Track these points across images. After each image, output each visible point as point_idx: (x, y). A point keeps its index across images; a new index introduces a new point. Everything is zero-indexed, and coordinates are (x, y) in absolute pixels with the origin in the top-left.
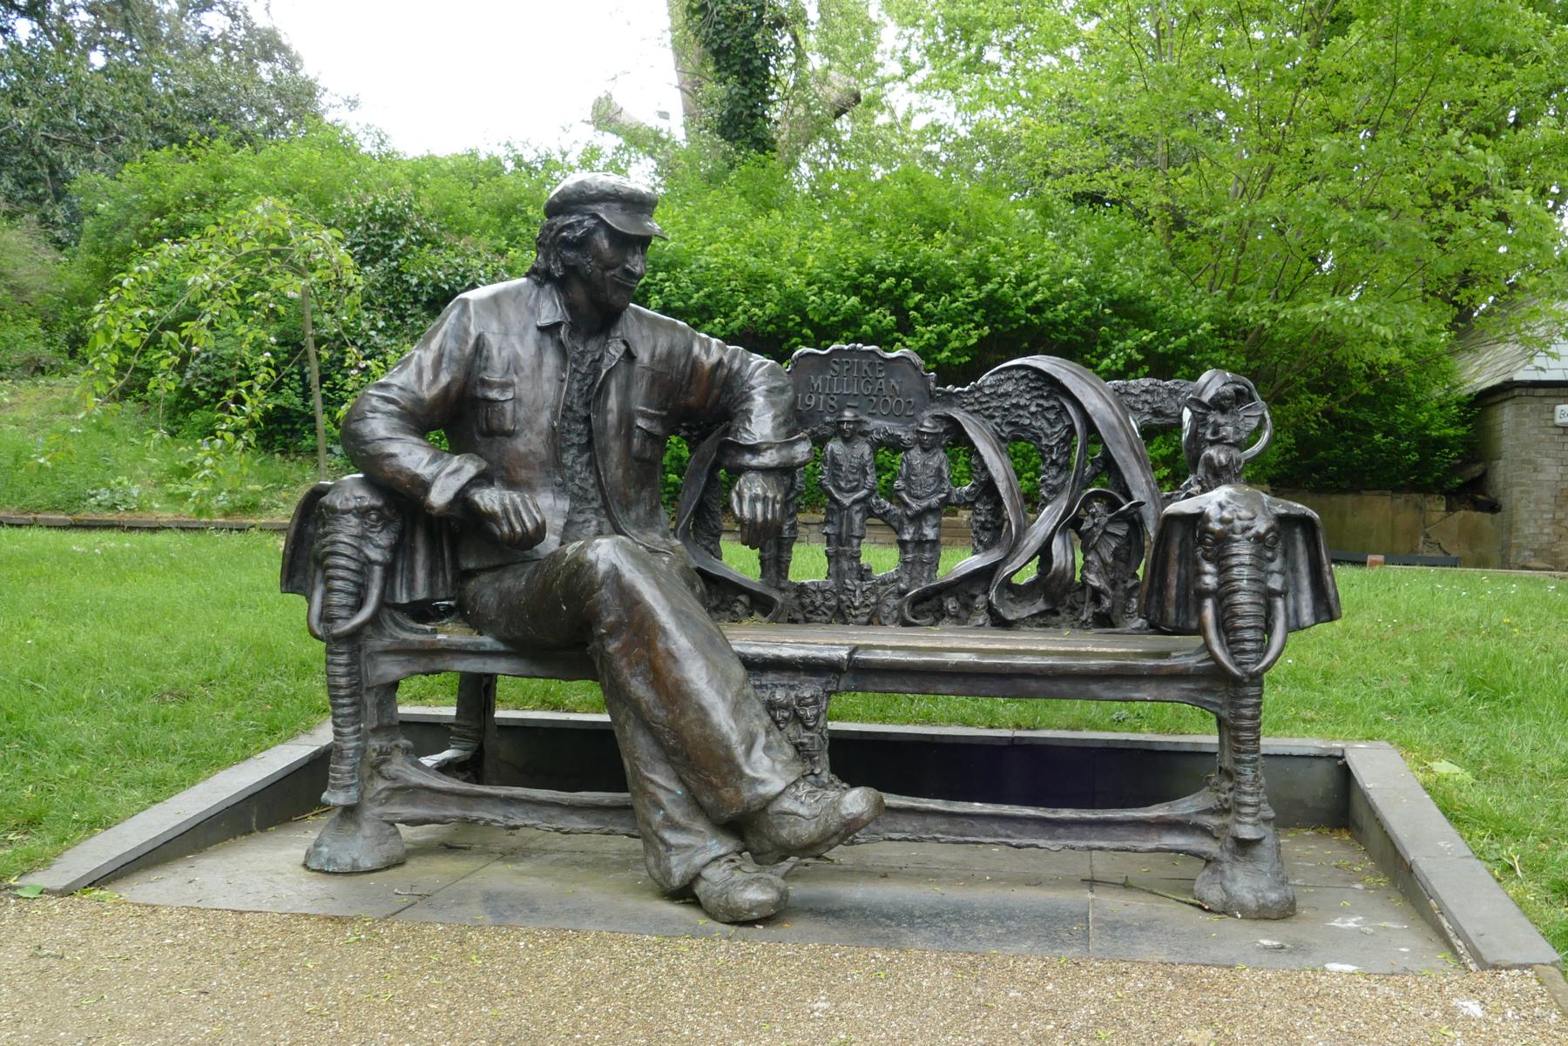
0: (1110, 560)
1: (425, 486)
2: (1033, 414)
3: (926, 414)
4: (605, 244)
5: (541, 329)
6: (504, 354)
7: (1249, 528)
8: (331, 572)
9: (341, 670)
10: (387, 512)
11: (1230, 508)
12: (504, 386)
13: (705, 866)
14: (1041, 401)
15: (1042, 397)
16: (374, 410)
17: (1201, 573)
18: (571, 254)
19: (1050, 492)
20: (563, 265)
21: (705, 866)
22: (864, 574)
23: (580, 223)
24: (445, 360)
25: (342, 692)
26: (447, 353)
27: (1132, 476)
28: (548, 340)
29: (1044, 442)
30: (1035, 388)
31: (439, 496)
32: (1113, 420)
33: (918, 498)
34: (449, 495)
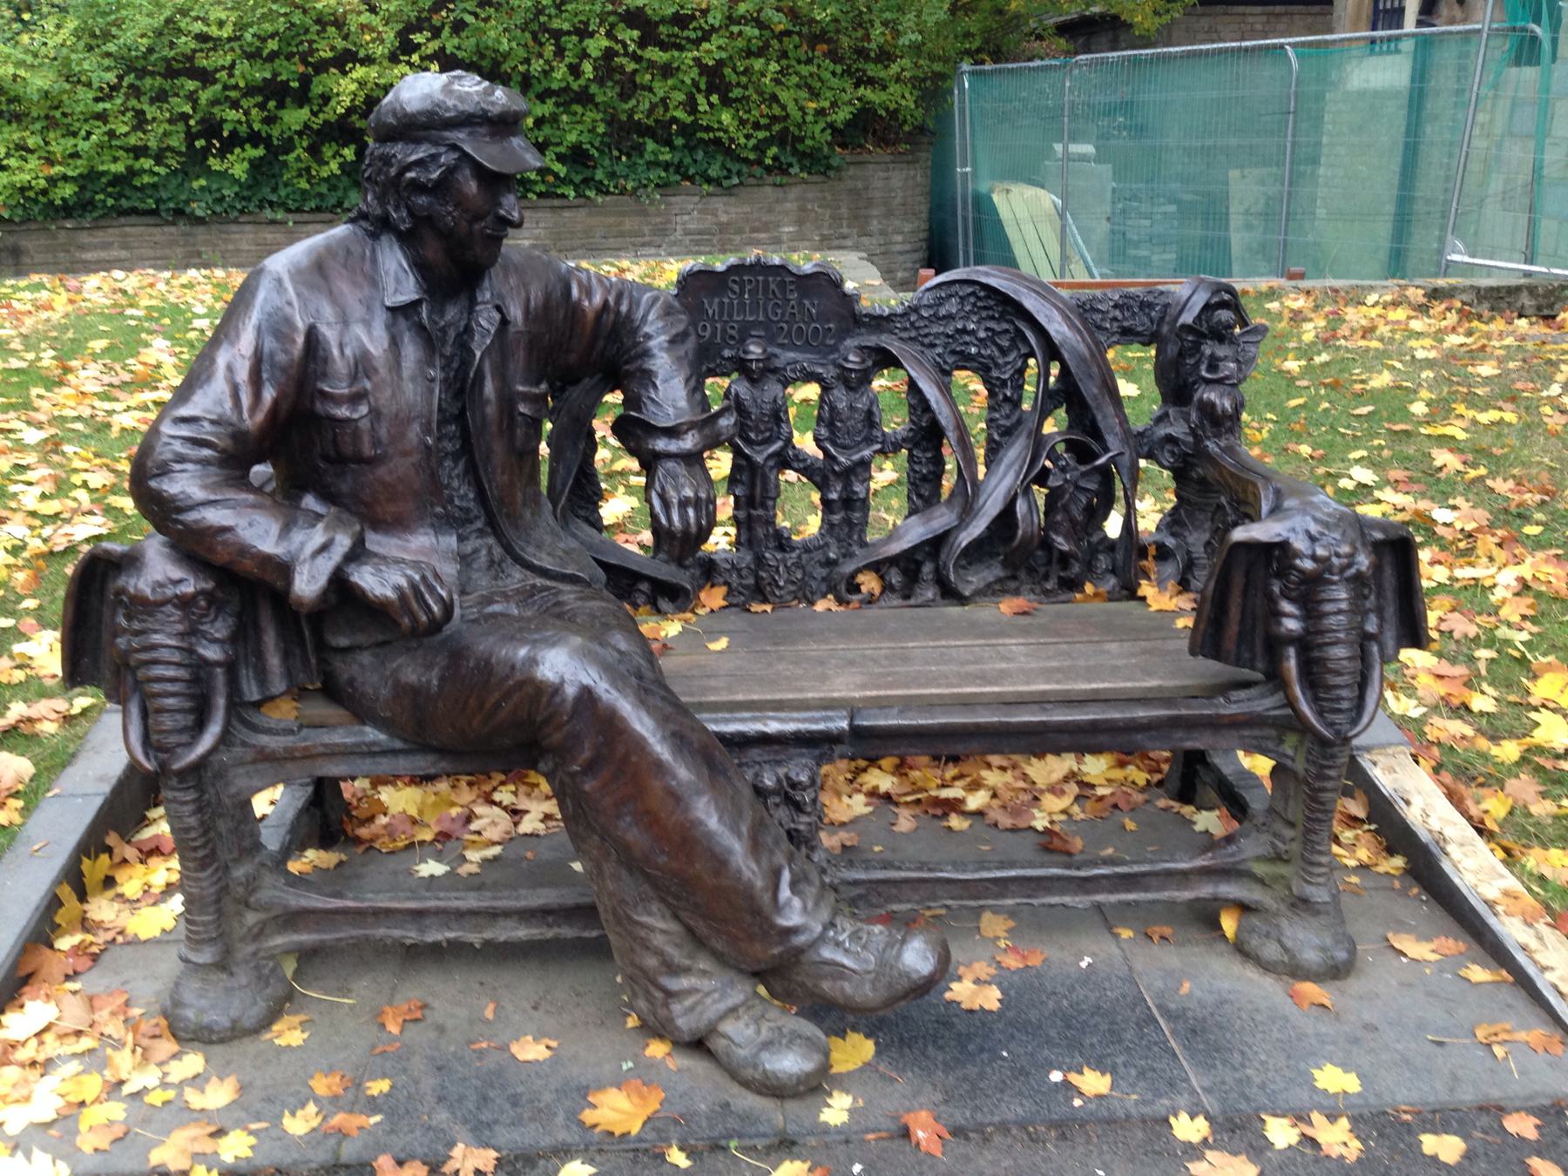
0: (1080, 518)
1: (285, 569)
2: (980, 340)
3: (849, 343)
4: (472, 187)
5: (393, 310)
6: (348, 351)
7: (1349, 566)
8: (141, 674)
9: (188, 809)
10: (219, 594)
11: (1325, 540)
12: (356, 399)
13: (723, 1017)
14: (992, 324)
15: (992, 318)
16: (181, 459)
17: (1279, 615)
18: (422, 200)
19: (1001, 435)
20: (411, 214)
21: (723, 1017)
22: (782, 542)
23: (434, 157)
24: (265, 366)
25: (193, 835)
26: (265, 357)
27: (1105, 417)
28: (403, 323)
29: (995, 373)
30: (985, 308)
31: (308, 584)
32: (1082, 348)
33: (845, 447)
34: (322, 581)
